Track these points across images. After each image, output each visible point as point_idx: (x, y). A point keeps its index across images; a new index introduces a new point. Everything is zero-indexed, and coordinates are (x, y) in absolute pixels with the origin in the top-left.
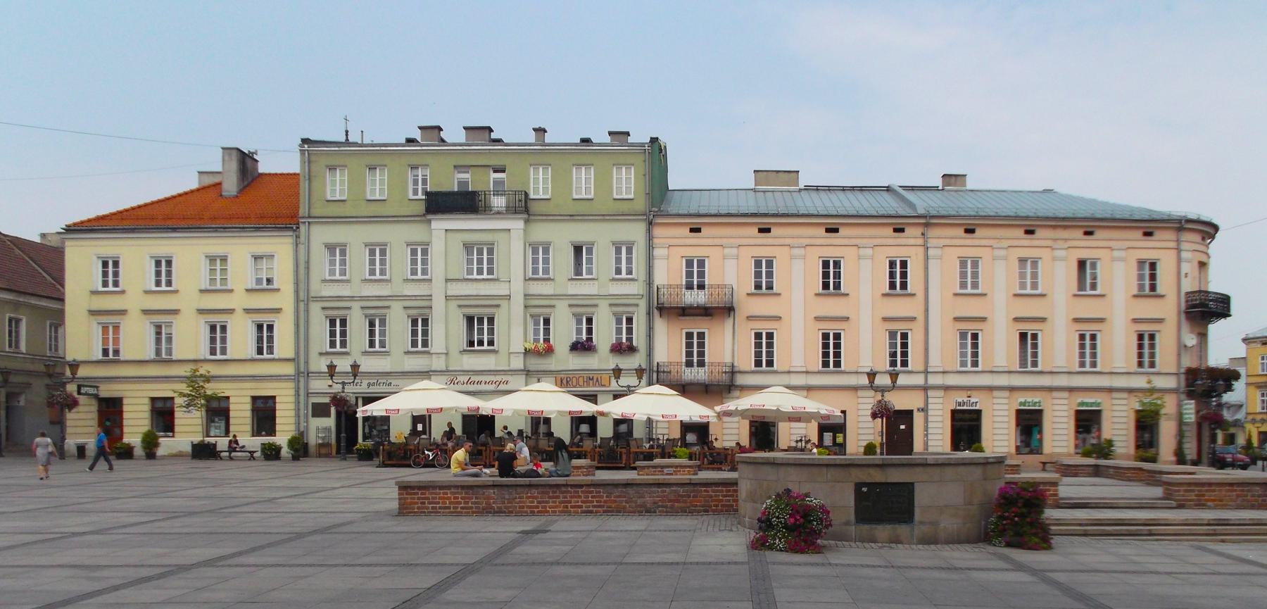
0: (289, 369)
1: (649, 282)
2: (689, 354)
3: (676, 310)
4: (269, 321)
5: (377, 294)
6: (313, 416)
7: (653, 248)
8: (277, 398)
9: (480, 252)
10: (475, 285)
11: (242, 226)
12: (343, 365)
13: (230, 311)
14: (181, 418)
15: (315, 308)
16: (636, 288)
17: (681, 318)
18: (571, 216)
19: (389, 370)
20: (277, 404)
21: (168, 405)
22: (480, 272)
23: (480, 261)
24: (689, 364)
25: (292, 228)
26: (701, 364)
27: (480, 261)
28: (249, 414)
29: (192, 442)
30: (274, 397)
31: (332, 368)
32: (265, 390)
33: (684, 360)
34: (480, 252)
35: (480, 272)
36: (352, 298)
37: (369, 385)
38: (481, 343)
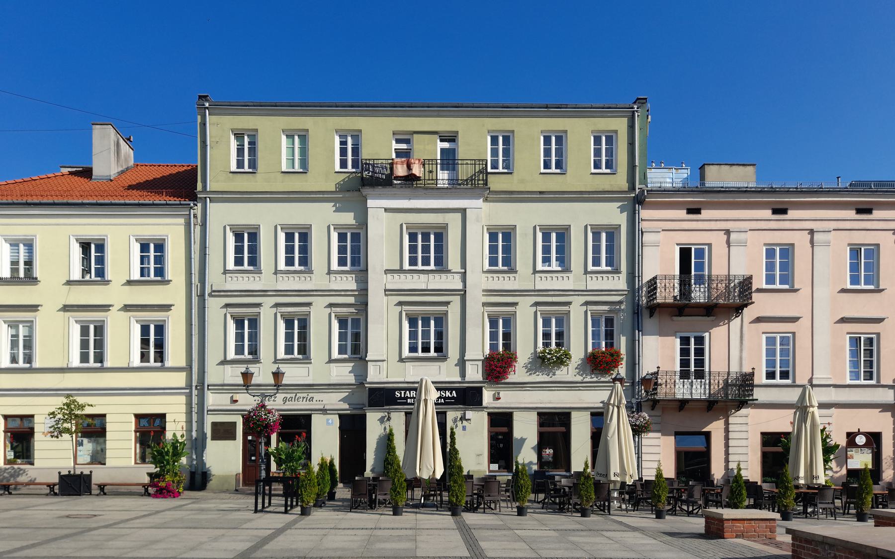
0: (179, 379)
1: (633, 275)
2: (685, 363)
3: (670, 309)
4: (107, 321)
5: (297, 288)
6: (213, 438)
7: (642, 232)
8: (167, 416)
9: (426, 237)
10: (423, 277)
11: (122, 202)
12: (262, 375)
13: (105, 308)
14: (42, 444)
15: (214, 306)
16: (620, 283)
17: (675, 318)
18: (541, 193)
19: (311, 382)
20: (167, 423)
21: (26, 424)
22: (426, 262)
23: (426, 249)
24: (685, 375)
25: (189, 205)
26: (700, 375)
27: (426, 249)
28: (133, 436)
29: (59, 473)
30: (163, 416)
31: (247, 376)
32: (151, 405)
33: (678, 368)
34: (426, 237)
35: (426, 262)
36: (264, 293)
37: (285, 400)
38: (426, 349)
